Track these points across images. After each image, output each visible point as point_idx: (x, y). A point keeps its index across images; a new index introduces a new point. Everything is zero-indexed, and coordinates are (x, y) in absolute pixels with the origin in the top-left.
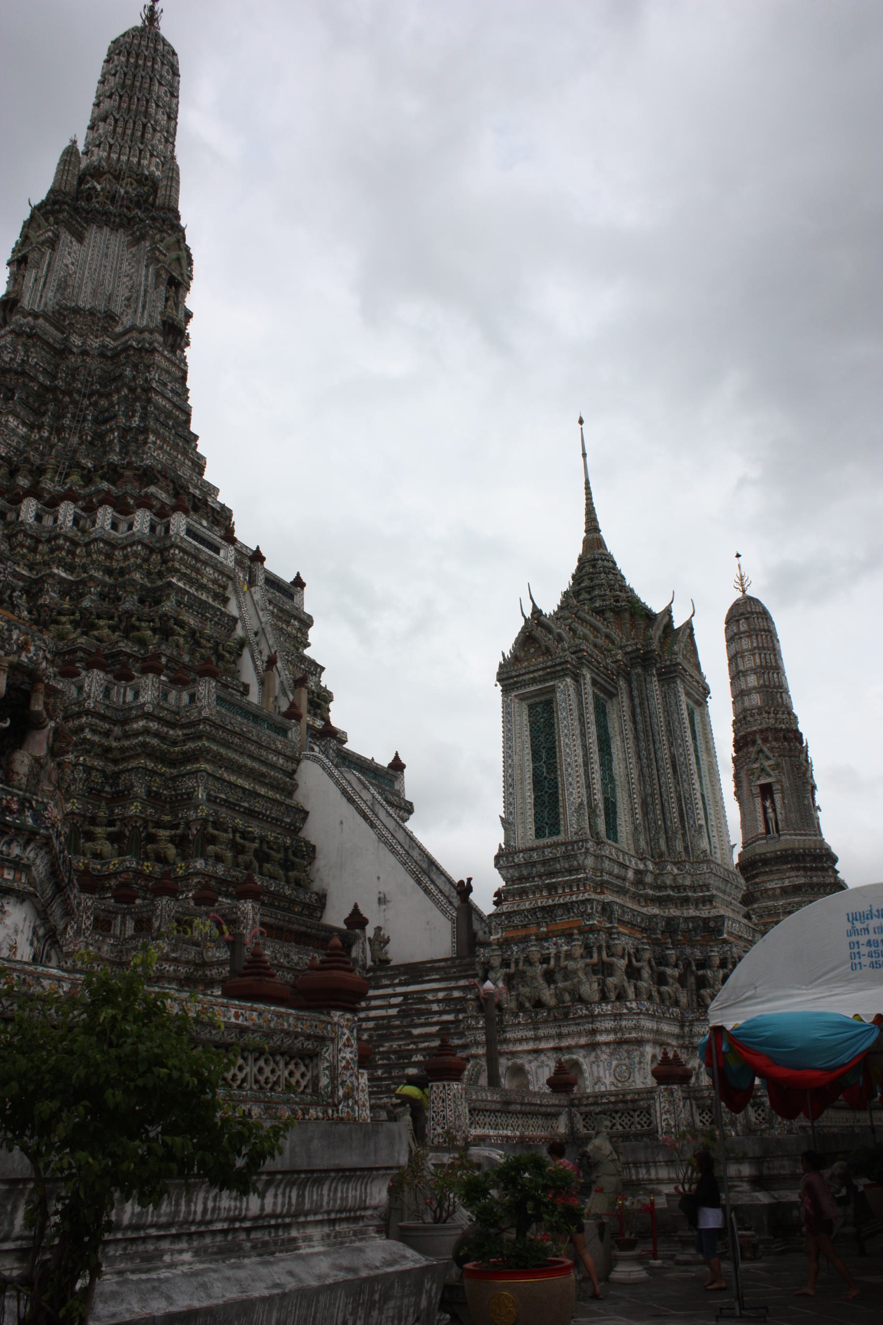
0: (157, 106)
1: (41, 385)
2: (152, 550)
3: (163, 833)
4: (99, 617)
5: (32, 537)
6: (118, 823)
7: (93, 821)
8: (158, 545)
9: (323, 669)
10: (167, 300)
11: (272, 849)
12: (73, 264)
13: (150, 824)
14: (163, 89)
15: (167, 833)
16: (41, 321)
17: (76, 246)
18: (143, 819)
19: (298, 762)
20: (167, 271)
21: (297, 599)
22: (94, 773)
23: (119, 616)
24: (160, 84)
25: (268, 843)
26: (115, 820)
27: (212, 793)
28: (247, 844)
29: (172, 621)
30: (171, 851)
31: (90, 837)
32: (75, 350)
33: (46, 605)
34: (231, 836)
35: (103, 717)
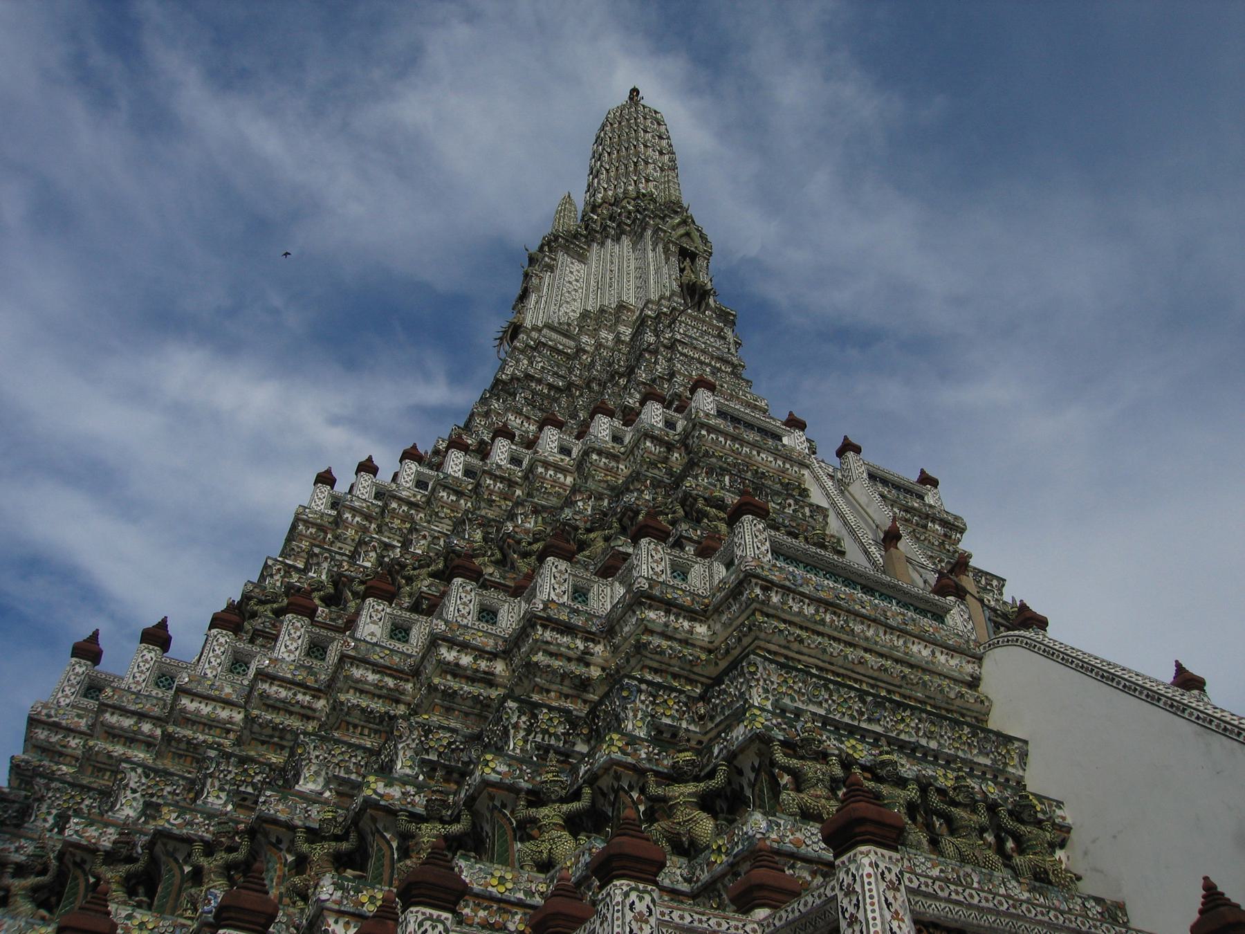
0: (646, 146)
1: (551, 386)
2: (670, 447)
3: (683, 791)
4: (589, 531)
5: (502, 479)
6: (587, 791)
7: (537, 798)
8: (677, 438)
9: (1002, 581)
10: (682, 270)
11: (956, 804)
12: (577, 281)
13: (651, 778)
14: (649, 136)
15: (691, 788)
16: (545, 331)
17: (577, 266)
18: (634, 768)
19: (979, 659)
20: (675, 244)
21: (929, 499)
22: (543, 715)
23: (620, 521)
24: (645, 132)
25: (941, 792)
26: (580, 788)
27: (787, 701)
28: (885, 789)
29: (701, 501)
30: (705, 825)
31: (527, 829)
32: (588, 348)
33: (509, 535)
34: (838, 771)
35: (567, 629)
